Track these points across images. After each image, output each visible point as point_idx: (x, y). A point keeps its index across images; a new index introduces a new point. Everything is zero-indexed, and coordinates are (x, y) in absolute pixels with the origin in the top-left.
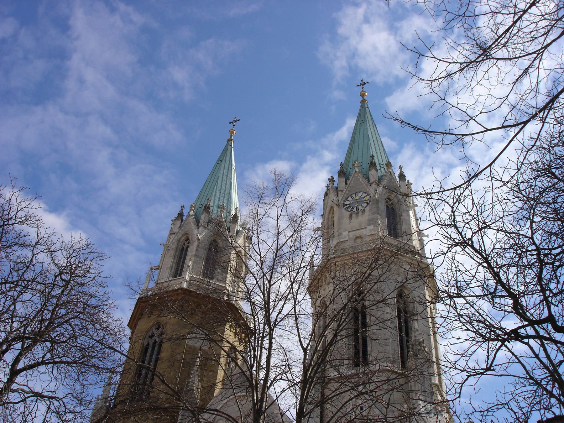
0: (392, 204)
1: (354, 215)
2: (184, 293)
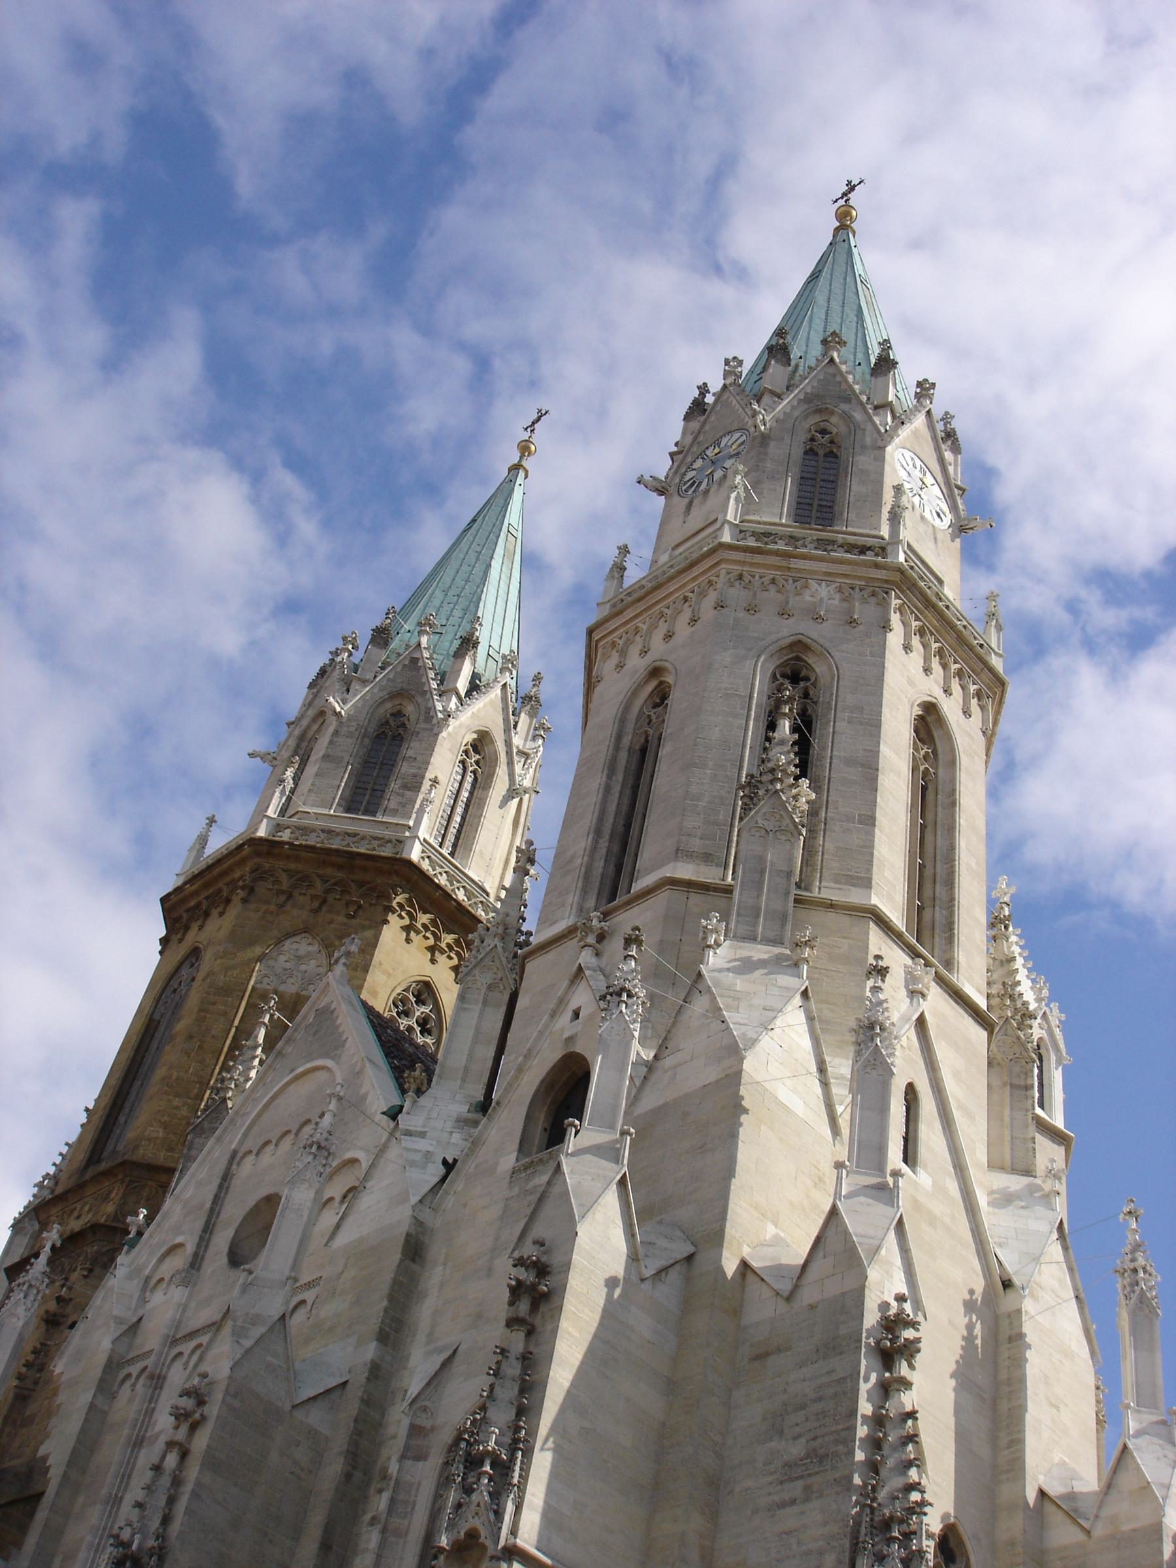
0: (832, 442)
1: (696, 502)
2: (258, 854)
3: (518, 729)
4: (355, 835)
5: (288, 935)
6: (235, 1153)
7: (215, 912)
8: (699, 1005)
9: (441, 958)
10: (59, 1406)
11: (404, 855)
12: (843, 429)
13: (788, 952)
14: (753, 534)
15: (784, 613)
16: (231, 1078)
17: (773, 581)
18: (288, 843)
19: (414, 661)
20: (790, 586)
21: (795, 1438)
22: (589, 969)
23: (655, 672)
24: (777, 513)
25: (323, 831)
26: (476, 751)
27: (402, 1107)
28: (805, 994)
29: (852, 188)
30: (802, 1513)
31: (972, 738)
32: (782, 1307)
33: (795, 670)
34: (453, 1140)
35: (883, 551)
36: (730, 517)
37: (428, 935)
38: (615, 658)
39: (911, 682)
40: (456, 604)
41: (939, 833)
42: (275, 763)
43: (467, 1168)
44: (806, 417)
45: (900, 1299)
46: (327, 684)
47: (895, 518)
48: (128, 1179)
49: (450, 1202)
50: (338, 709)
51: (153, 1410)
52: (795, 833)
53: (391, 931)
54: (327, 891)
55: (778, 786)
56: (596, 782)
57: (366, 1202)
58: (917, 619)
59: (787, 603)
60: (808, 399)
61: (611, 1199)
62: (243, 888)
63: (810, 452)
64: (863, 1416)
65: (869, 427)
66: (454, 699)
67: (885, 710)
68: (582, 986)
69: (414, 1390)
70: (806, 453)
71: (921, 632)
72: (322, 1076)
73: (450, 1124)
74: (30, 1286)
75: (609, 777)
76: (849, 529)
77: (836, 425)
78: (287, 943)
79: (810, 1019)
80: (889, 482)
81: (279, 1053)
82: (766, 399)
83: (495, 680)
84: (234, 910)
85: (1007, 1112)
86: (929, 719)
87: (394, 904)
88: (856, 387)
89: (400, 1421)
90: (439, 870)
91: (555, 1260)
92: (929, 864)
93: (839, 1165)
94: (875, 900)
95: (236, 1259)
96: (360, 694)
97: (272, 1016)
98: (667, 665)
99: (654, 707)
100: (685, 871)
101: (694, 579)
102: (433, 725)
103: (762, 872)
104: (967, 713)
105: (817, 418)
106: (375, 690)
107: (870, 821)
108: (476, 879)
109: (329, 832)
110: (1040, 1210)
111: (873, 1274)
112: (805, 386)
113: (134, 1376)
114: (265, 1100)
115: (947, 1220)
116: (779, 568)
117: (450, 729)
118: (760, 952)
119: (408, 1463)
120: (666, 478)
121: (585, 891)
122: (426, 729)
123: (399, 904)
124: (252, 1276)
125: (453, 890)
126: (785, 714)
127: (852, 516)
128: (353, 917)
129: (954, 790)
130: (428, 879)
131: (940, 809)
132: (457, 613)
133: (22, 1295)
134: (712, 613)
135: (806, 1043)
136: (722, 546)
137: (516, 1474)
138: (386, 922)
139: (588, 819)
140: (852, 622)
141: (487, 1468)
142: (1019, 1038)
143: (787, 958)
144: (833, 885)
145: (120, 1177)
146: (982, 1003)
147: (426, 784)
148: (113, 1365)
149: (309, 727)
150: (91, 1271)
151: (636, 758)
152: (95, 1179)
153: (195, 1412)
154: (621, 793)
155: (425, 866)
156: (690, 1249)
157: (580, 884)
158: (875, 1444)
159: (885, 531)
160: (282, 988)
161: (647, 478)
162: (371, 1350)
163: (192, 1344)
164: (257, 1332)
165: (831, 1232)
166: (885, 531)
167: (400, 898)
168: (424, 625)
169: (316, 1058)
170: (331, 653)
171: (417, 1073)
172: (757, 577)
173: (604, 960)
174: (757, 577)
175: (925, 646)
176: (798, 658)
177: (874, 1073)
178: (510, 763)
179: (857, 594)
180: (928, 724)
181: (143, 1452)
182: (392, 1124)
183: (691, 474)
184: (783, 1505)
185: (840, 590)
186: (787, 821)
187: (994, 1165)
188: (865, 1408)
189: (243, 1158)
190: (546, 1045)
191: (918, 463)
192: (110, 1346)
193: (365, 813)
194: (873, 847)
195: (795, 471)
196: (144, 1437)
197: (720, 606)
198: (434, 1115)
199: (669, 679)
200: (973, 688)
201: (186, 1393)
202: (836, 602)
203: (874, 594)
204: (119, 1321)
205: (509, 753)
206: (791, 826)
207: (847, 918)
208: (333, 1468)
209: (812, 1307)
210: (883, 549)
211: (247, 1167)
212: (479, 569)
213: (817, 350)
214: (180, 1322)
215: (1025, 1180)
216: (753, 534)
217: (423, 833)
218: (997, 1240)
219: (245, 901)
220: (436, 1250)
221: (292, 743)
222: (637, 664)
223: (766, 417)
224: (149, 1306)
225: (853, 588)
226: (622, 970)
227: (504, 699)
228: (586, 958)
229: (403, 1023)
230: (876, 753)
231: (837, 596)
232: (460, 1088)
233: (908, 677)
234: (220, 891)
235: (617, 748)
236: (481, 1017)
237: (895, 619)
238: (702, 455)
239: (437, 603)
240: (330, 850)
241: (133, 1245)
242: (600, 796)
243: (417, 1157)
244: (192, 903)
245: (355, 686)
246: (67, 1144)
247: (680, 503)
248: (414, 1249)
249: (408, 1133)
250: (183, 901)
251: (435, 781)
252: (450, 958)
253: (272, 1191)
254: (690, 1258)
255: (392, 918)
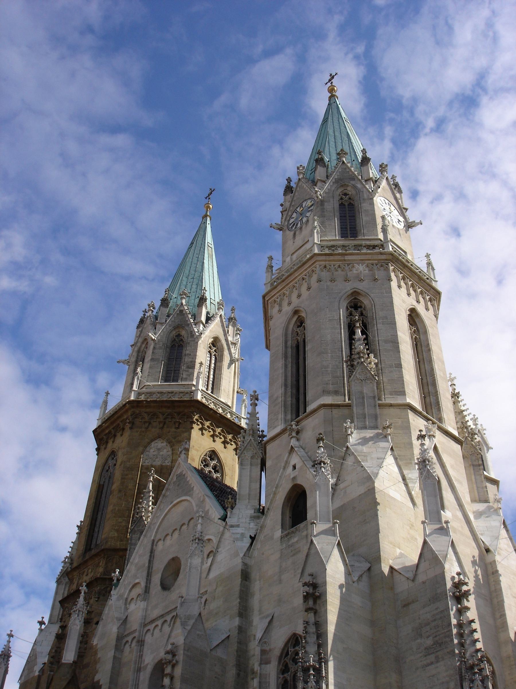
0: (350, 199)
1: (297, 233)
2: (133, 407)
3: (229, 333)
4: (172, 393)
5: (152, 441)
6: (153, 540)
7: (118, 435)
8: (350, 461)
9: (217, 439)
10: (99, 658)
11: (195, 398)
12: (354, 192)
13: (380, 431)
14: (327, 247)
15: (346, 280)
16: (143, 507)
17: (339, 266)
18: (145, 401)
19: (181, 311)
20: (347, 268)
21: (428, 637)
22: (296, 447)
23: (296, 312)
24: (334, 235)
25: (158, 393)
26: (214, 346)
27: (227, 515)
28: (392, 449)
29: (333, 77)
30: (437, 667)
31: (431, 320)
32: (411, 584)
33: (355, 305)
34: (251, 527)
35: (382, 246)
36: (316, 241)
37: (210, 430)
38: (277, 308)
39: (404, 302)
40: (193, 282)
41: (426, 363)
42: (129, 364)
43: (261, 538)
44: (337, 188)
45: (459, 574)
46: (145, 326)
47: (384, 230)
48: (106, 556)
49: (256, 553)
50: (153, 338)
51: (142, 655)
52: (374, 380)
53: (195, 432)
54: (165, 419)
55: (362, 360)
56: (280, 364)
57: (220, 557)
58: (401, 273)
59: (347, 275)
60: (337, 181)
61: (336, 552)
62: (129, 423)
63: (342, 205)
64: (454, 625)
65: (365, 190)
66: (201, 326)
67: (396, 316)
68: (294, 455)
69: (259, 635)
70: (340, 205)
71: (404, 278)
72: (185, 504)
73: (248, 519)
74: (79, 611)
75: (285, 361)
76: (366, 237)
77: (350, 191)
78: (153, 444)
79: (396, 459)
80: (378, 214)
81: (164, 495)
82: (319, 184)
83: (217, 314)
84: (127, 433)
85: (473, 477)
86: (413, 315)
87: (194, 420)
88: (356, 173)
89: (255, 648)
90: (210, 402)
91: (319, 581)
92: (424, 378)
93: (423, 523)
94: (408, 400)
95: (165, 587)
96: (161, 329)
97: (153, 477)
98: (301, 309)
99: (298, 327)
100: (328, 400)
101: (306, 270)
102: (195, 339)
103: (363, 398)
104: (427, 309)
105: (342, 189)
106: (168, 327)
107: (399, 366)
108: (224, 401)
109: (161, 393)
110: (494, 517)
111: (447, 566)
112: (335, 176)
113: (130, 641)
114: (162, 517)
115: (460, 529)
116: (340, 261)
117: (202, 339)
118: (369, 433)
119: (263, 666)
120: (282, 223)
121: (285, 412)
122: (192, 341)
123: (196, 419)
124: (183, 599)
125: (217, 409)
126: (358, 327)
127: (365, 231)
128: (178, 428)
129: (428, 344)
130: (207, 407)
131: (424, 353)
132: (194, 286)
133: (76, 615)
134: (317, 284)
135: (396, 469)
136: (315, 255)
137: (324, 672)
138: (192, 428)
139: (280, 381)
140: (375, 280)
141: (312, 672)
142: (472, 445)
143: (381, 434)
144: (390, 396)
145: (103, 555)
146: (456, 433)
147: (197, 366)
148: (120, 638)
149: (141, 346)
150: (99, 598)
151: (294, 351)
152: (92, 558)
153: (173, 660)
154: (292, 367)
155: (204, 401)
156: (369, 565)
157: (283, 410)
158: (461, 635)
159: (381, 236)
160: (154, 464)
161: (274, 224)
162: (237, 621)
163: (153, 625)
164: (191, 622)
165: (425, 550)
166: (381, 236)
167: (196, 417)
168: (183, 295)
169: (180, 497)
170: (143, 311)
171: (230, 500)
172: (332, 266)
173: (301, 442)
174: (332, 266)
175: (406, 284)
176: (355, 299)
177: (429, 480)
178: (229, 349)
179: (375, 267)
180: (413, 317)
181: (141, 673)
182: (224, 523)
183: (292, 221)
184: (428, 665)
185: (367, 266)
186: (369, 375)
187: (473, 501)
188: (454, 621)
189: (157, 542)
190: (284, 482)
191: (387, 201)
192: (117, 630)
193: (173, 381)
194: (403, 377)
195: (337, 214)
196: (140, 667)
197: (319, 281)
198: (241, 517)
199: (303, 315)
200: (428, 298)
201: (167, 653)
202: (367, 272)
203: (382, 266)
204: (118, 619)
205: (228, 345)
206: (371, 376)
207: (399, 409)
208: (231, 672)
209: (424, 583)
210: (382, 245)
211: (160, 546)
212: (199, 264)
213: (334, 157)
214: (145, 616)
215: (486, 505)
216: (327, 247)
217: (200, 387)
218: (480, 532)
219: (131, 428)
220: (255, 575)
221: (135, 354)
222: (287, 309)
223: (320, 192)
224: (129, 611)
225: (373, 265)
226: (318, 453)
227: (222, 321)
228: (293, 442)
229: (207, 469)
230: (396, 336)
231: (367, 269)
232: (249, 502)
233: (402, 299)
234: (119, 424)
235: (286, 347)
236: (251, 471)
237: (393, 275)
238: (295, 211)
239: (184, 283)
240: (163, 401)
241: (116, 585)
242: (283, 370)
243: (238, 536)
244: (107, 431)
245: (158, 326)
246: (72, 542)
247: (290, 234)
248: (246, 575)
249: (232, 526)
250: (103, 431)
251: (201, 364)
252: (221, 438)
253: (174, 556)
254: (369, 569)
255: (195, 426)
